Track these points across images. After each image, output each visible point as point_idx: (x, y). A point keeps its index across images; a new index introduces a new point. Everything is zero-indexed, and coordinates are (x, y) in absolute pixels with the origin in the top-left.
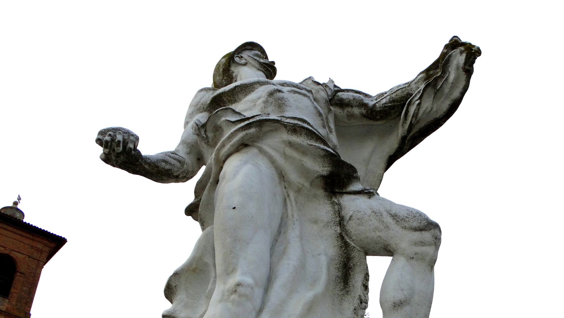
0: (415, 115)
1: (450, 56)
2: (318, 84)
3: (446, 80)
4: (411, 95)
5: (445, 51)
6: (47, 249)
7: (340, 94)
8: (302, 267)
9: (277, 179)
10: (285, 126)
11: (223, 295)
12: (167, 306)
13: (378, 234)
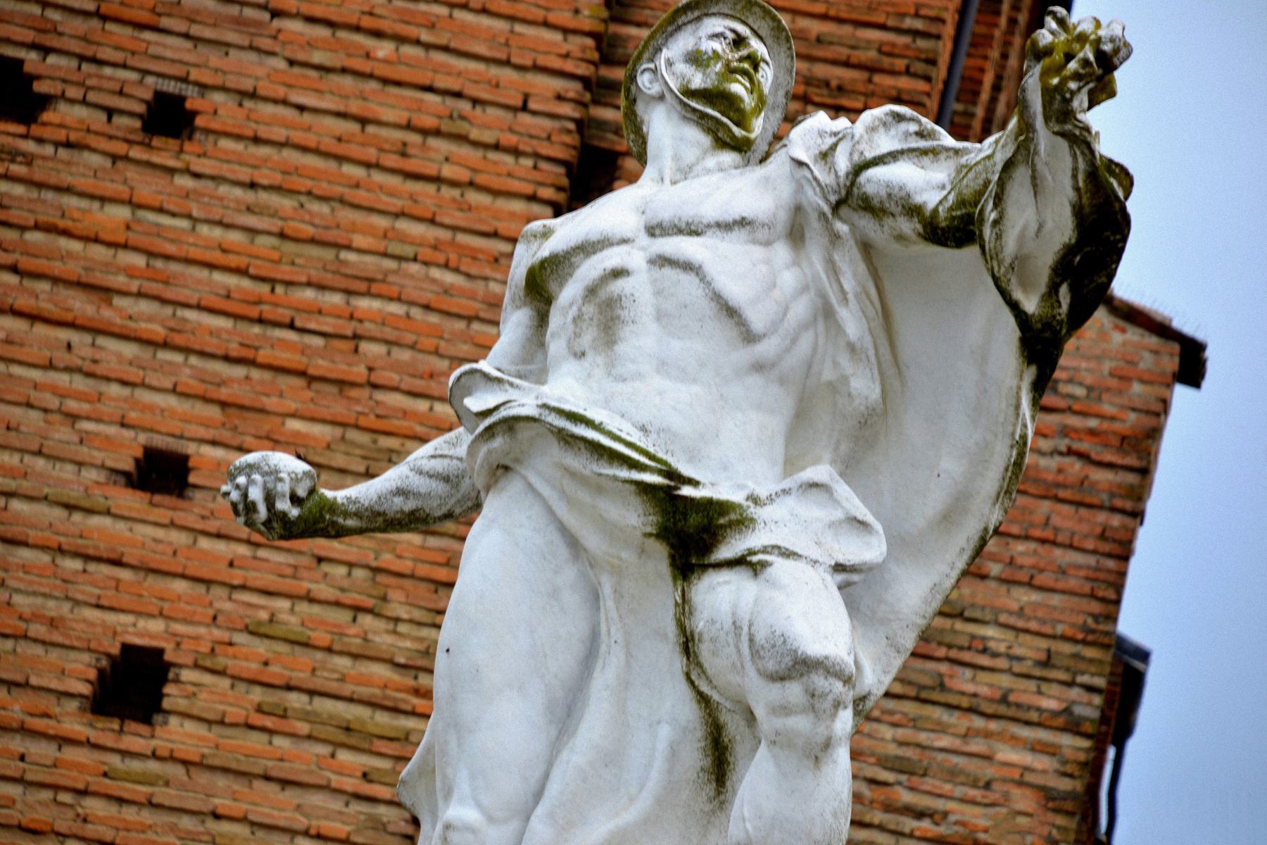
9: (563, 551)
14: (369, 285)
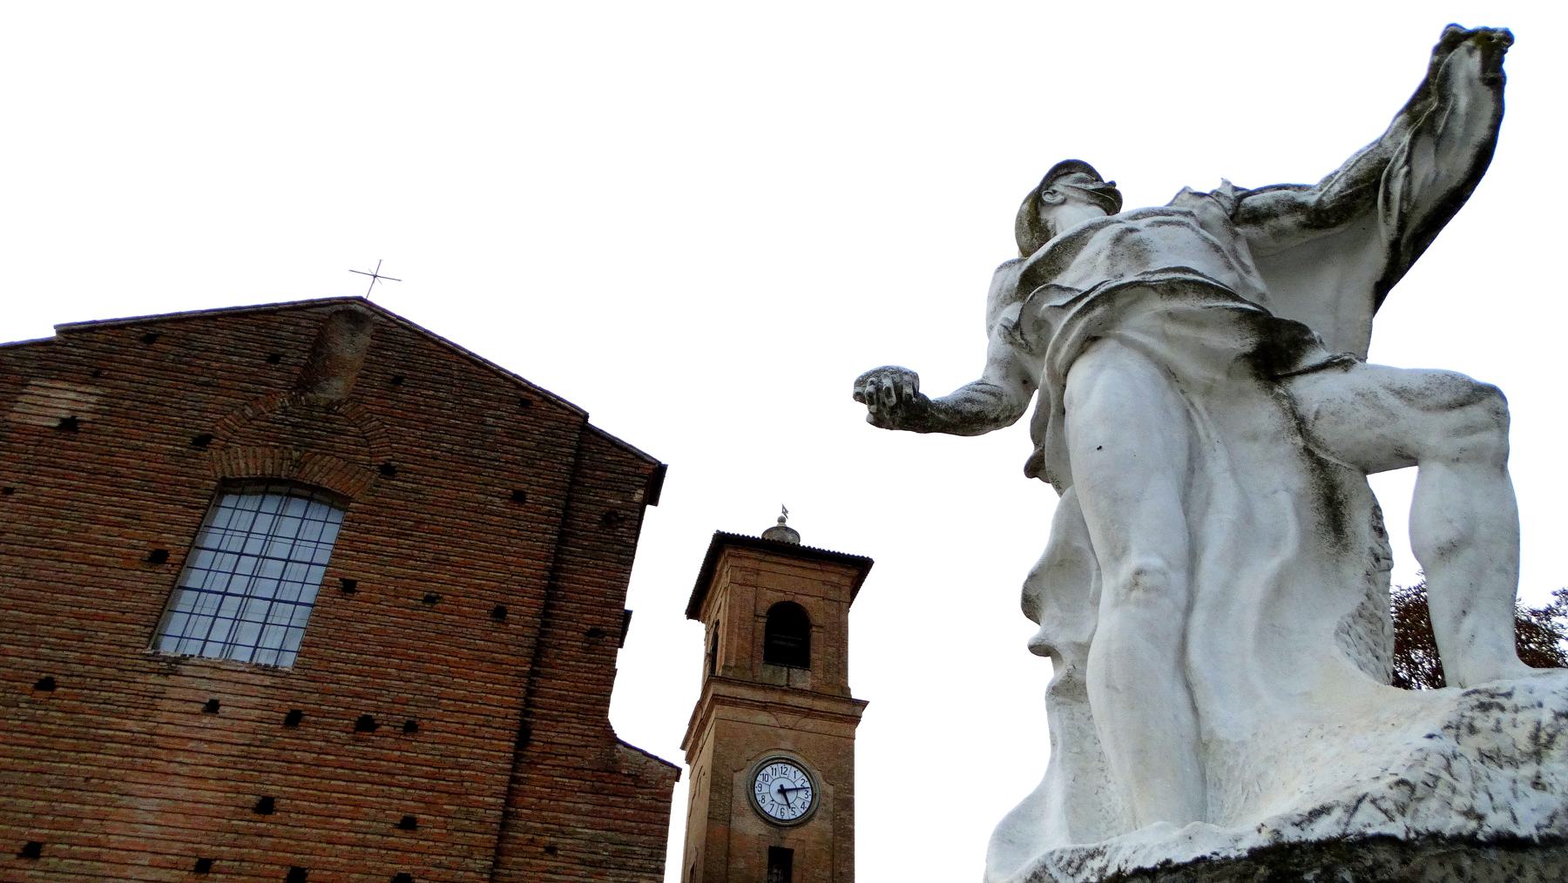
0: (1406, 195)
1: (1448, 66)
2: (1202, 195)
3: (1453, 112)
4: (1388, 161)
5: (1436, 58)
6: (847, 581)
7: (1247, 200)
8: (1247, 517)
9: (1163, 382)
10: (1154, 288)
11: (1118, 594)
12: (1032, 630)
13: (1377, 431)
14: (466, 767)
